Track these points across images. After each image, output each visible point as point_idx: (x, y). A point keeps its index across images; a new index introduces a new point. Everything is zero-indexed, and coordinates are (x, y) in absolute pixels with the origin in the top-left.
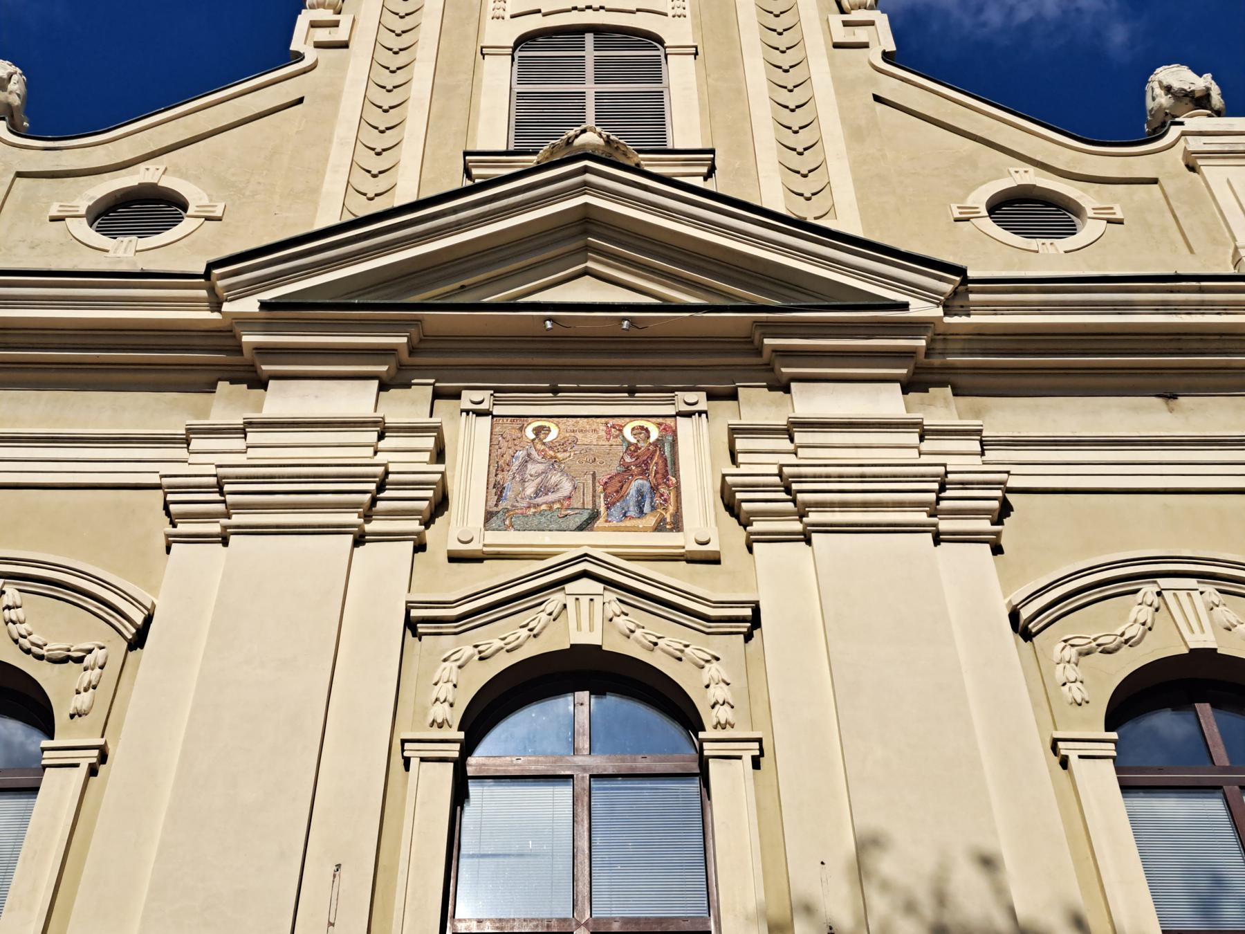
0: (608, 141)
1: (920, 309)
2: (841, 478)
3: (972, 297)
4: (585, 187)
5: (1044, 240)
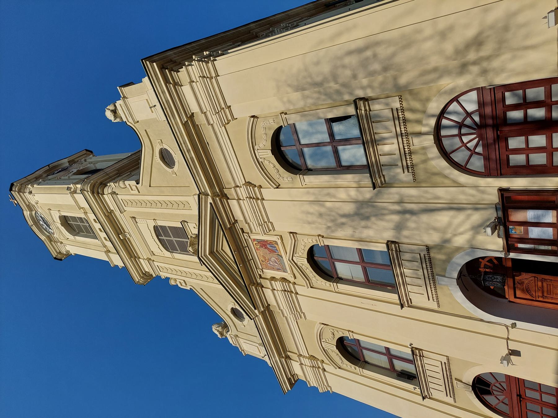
0: (190, 246)
1: (210, 200)
2: (256, 216)
3: (203, 191)
4: (205, 255)
5: (174, 158)
